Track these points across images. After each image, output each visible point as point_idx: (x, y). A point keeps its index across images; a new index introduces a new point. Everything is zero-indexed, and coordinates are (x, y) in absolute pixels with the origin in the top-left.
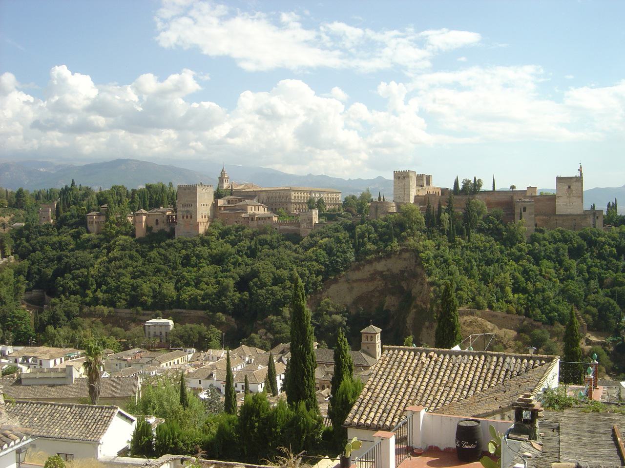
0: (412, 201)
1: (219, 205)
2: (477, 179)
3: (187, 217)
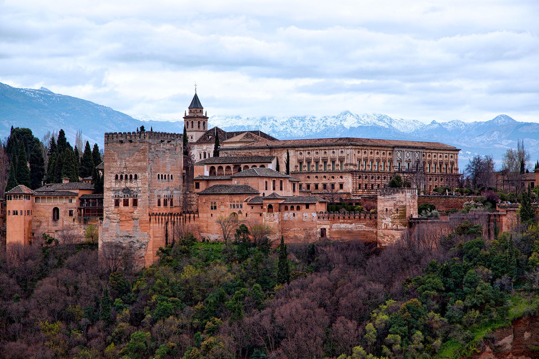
1: (196, 176)
3: (126, 204)
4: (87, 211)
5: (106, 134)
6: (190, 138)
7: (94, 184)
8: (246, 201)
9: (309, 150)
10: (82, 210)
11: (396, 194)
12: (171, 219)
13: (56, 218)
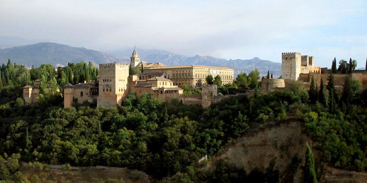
0: (297, 76)
1: (134, 80)
2: (352, 60)
3: (107, 90)
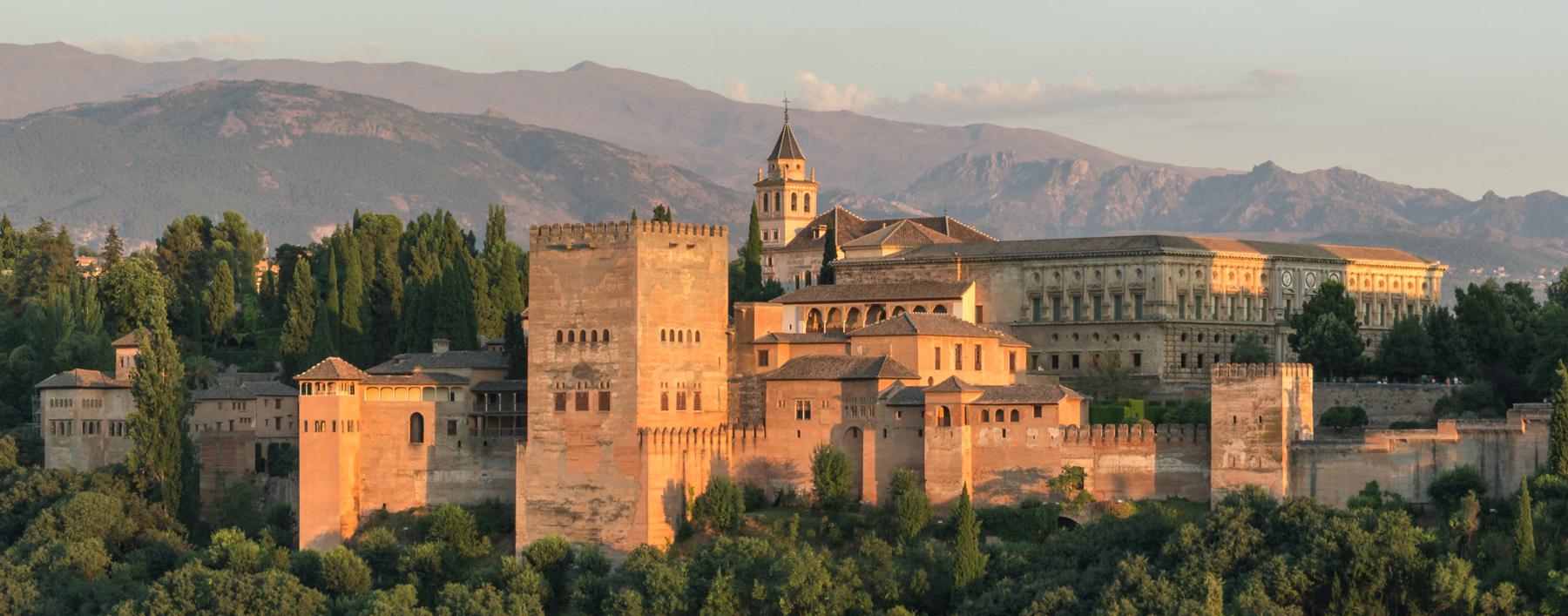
1: (760, 333)
3: (582, 404)
4: (492, 419)
5: (533, 228)
6: (772, 236)
7: (509, 356)
8: (884, 397)
9: (1055, 267)
10: (480, 420)
11: (1257, 381)
12: (695, 442)
13: (417, 437)
